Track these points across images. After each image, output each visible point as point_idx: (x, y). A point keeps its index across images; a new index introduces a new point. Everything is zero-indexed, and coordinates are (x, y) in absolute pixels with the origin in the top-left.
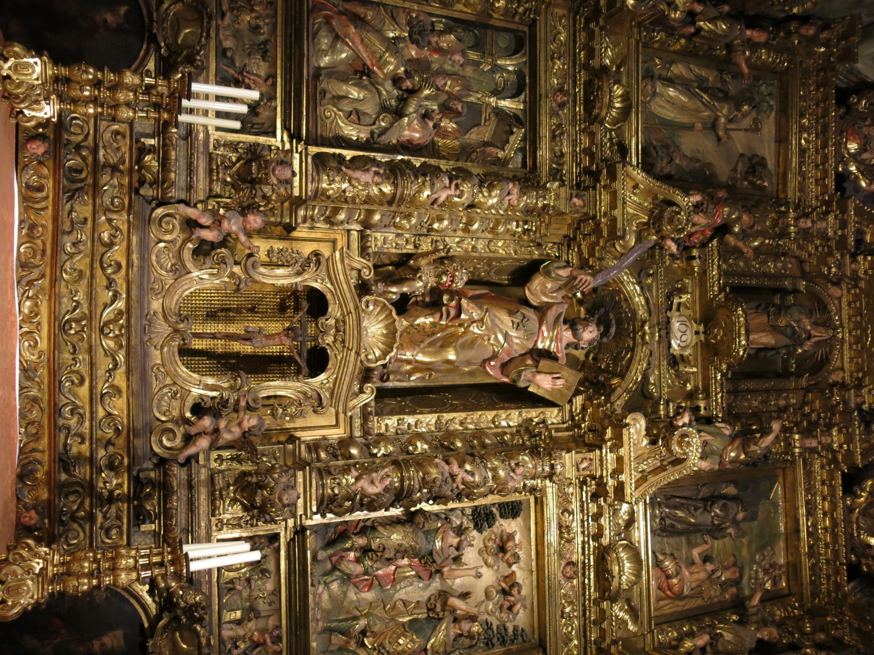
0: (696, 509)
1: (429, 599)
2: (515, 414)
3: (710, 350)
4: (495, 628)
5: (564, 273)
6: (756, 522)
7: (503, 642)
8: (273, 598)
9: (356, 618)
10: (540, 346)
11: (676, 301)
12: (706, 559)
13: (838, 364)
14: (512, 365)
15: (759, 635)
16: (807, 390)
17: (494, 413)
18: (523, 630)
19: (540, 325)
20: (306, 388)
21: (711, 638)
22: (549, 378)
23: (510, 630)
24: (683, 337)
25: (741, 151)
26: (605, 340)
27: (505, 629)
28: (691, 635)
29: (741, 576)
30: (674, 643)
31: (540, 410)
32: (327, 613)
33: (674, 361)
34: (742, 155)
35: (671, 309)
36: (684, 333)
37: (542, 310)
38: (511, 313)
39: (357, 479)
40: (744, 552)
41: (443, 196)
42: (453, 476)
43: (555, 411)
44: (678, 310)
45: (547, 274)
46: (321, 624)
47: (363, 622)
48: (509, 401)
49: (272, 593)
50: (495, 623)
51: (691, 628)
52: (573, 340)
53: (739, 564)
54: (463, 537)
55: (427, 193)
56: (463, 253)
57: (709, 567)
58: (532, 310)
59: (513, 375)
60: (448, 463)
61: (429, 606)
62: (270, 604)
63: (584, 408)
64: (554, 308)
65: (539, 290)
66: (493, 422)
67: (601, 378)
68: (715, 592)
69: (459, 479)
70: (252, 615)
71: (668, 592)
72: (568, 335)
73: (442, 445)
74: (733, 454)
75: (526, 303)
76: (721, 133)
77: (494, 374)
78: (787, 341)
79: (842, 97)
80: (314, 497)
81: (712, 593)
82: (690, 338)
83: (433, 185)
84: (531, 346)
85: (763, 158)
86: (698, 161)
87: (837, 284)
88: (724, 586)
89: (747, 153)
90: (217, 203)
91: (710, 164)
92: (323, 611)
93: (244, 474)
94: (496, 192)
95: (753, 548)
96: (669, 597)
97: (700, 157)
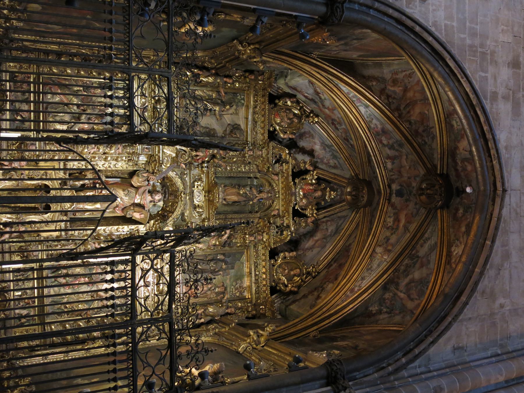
0: (204, 263)
2: (126, 227)
3: (210, 202)
5: (145, 175)
6: (234, 270)
10: (136, 202)
11: (196, 183)
13: (277, 207)
14: (126, 209)
16: (260, 218)
17: (117, 227)
19: (136, 194)
20: (42, 218)
22: (138, 214)
24: (199, 198)
25: (229, 123)
26: (165, 199)
31: (136, 226)
33: (195, 207)
34: (229, 124)
35: (194, 187)
36: (199, 196)
37: (137, 188)
38: (124, 190)
40: (228, 281)
41: (92, 151)
43: (143, 226)
44: (197, 187)
45: (138, 176)
48: (126, 223)
52: (152, 199)
53: (225, 285)
55: (86, 150)
56: (105, 169)
58: (134, 189)
59: (125, 213)
63: (154, 224)
64: (143, 188)
65: (135, 181)
66: (117, 230)
67: (166, 214)
68: (213, 296)
72: (149, 198)
73: (95, 238)
74: (214, 242)
75: (132, 186)
76: (218, 117)
77: (119, 213)
78: (244, 199)
79: (273, 99)
81: (212, 296)
82: (202, 198)
83: (88, 148)
84: (132, 202)
85: (239, 125)
86: (208, 128)
87: (277, 174)
88: (218, 294)
89: (231, 123)
90: (22, 88)
91: (214, 129)
93: (21, 246)
94: (114, 148)
95: (232, 280)
97: (209, 126)
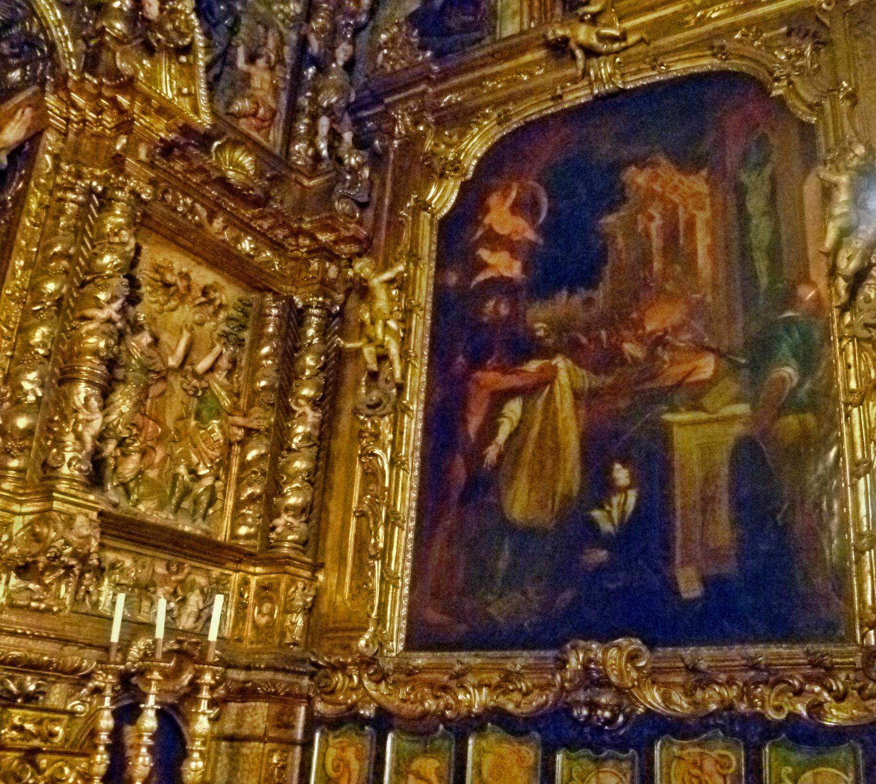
1: (185, 390)
4: (227, 329)
7: (243, 327)
8: (140, 562)
9: (176, 476)
12: (252, 59)
15: (341, 63)
18: (240, 300)
21: (329, 116)
23: (233, 312)
27: (232, 319)
28: (313, 130)
29: (280, 33)
30: (310, 152)
32: (161, 506)
39: (79, 437)
42: (109, 321)
46: (171, 517)
47: (182, 470)
49: (136, 562)
50: (224, 327)
51: (305, 124)
54: (147, 328)
57: (261, 62)
60: (90, 319)
61: (191, 393)
62: (144, 567)
69: (116, 316)
70: (152, 589)
71: (266, 124)
80: (80, 495)
92: (156, 509)
96: (269, 126)
